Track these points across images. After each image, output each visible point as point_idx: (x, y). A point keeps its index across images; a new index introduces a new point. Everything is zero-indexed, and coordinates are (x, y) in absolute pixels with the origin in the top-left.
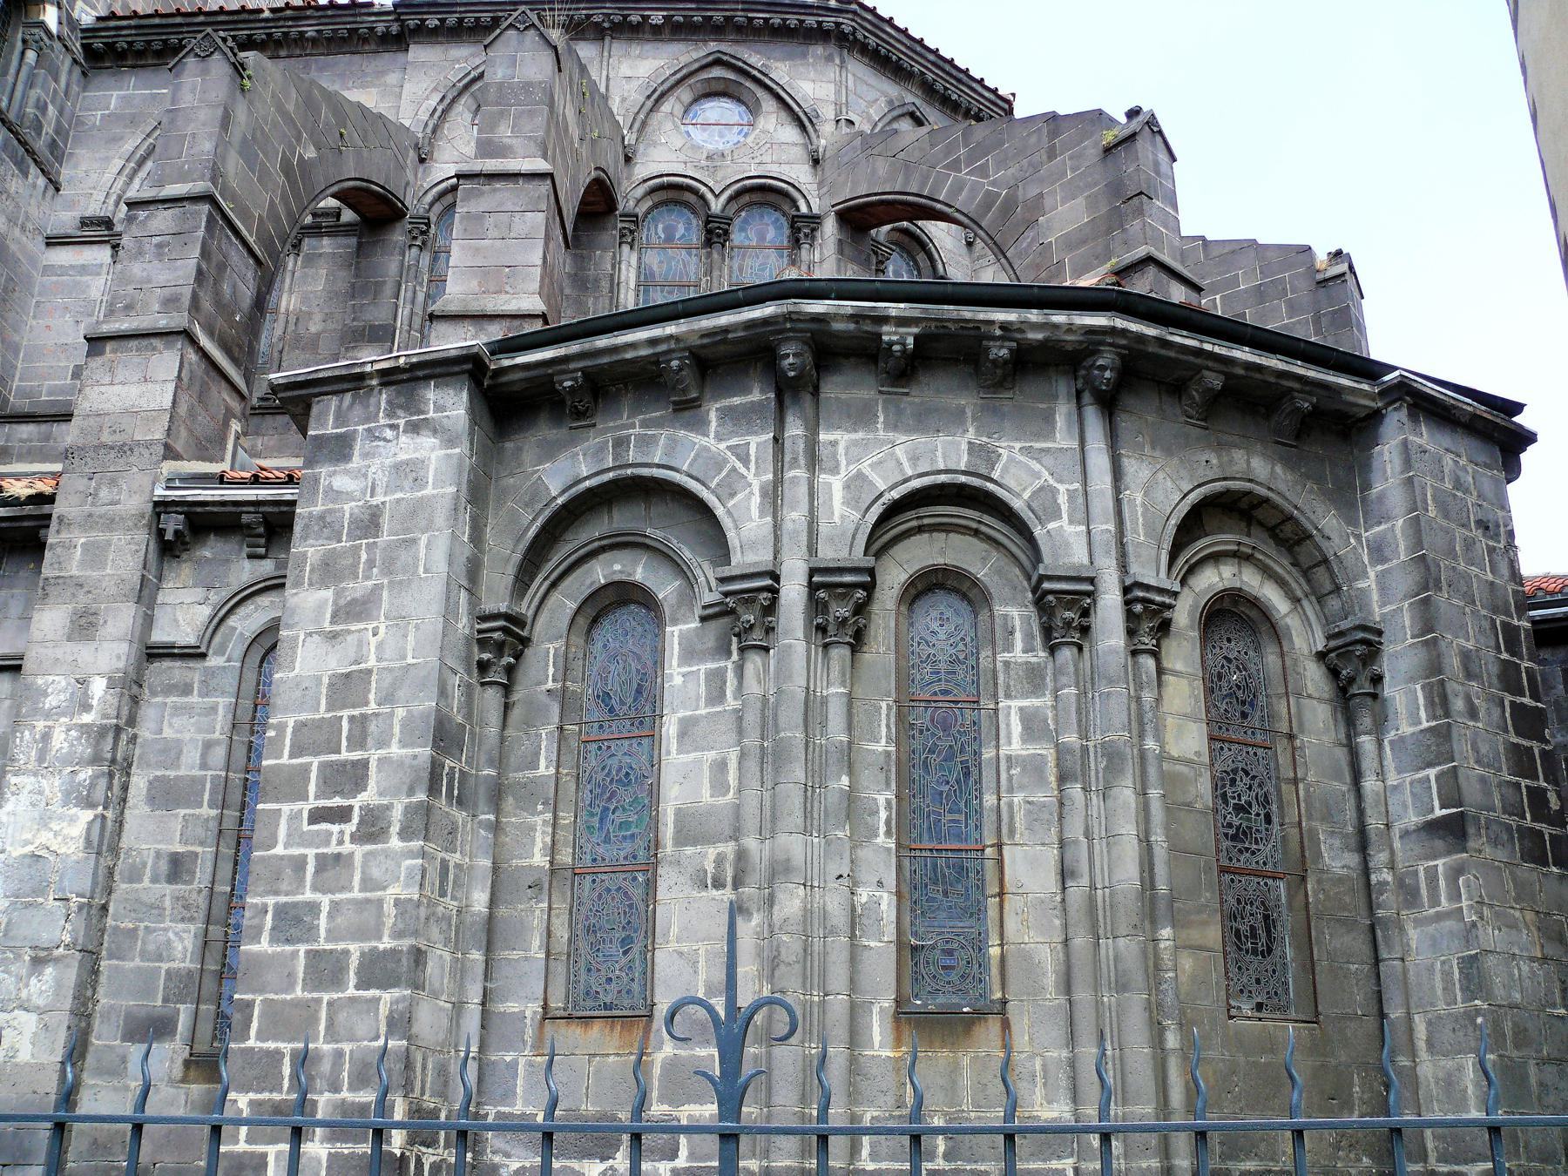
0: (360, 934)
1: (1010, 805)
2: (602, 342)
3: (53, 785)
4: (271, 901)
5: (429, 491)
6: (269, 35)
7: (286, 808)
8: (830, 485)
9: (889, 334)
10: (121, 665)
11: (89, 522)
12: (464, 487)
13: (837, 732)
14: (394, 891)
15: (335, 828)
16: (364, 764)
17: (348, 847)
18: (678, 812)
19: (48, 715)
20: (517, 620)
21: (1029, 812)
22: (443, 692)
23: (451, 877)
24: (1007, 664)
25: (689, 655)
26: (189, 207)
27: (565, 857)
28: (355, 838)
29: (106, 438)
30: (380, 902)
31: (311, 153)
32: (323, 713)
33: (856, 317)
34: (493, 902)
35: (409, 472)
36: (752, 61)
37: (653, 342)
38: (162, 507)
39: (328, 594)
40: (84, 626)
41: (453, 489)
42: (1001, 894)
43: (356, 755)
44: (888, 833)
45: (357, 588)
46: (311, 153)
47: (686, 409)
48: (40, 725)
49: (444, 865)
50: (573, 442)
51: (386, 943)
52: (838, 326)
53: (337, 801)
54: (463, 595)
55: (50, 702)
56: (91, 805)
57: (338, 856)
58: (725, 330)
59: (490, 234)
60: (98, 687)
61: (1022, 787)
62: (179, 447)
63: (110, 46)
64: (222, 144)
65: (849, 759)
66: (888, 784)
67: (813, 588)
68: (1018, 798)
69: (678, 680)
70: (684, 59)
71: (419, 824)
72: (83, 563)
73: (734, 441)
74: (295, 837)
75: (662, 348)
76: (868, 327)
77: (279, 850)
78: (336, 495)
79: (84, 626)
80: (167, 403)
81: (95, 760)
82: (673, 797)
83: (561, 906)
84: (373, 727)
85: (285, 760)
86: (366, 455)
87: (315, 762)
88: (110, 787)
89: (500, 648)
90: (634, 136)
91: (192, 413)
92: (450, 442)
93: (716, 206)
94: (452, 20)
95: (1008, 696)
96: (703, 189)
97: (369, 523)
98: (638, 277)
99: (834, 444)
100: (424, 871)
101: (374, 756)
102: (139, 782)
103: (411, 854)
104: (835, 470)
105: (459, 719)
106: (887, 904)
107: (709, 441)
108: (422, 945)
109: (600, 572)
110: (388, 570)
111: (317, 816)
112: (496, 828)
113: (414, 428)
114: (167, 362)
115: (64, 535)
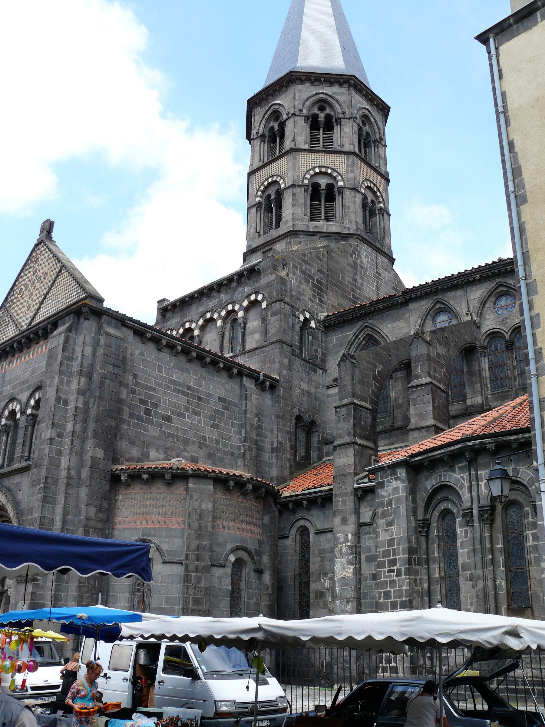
0: (399, 597)
1: (530, 557)
2: (430, 455)
3: (344, 560)
4: (382, 591)
5: (400, 495)
6: (370, 310)
7: (382, 570)
8: (481, 485)
9: (488, 446)
10: (354, 530)
11: (341, 495)
12: (408, 492)
13: (488, 545)
14: (404, 588)
15: (392, 574)
16: (396, 559)
17: (395, 578)
18: (462, 564)
19: (341, 544)
20: (427, 520)
21: (535, 559)
22: (409, 541)
23: (418, 582)
24: (528, 522)
25: (461, 527)
26: (348, 407)
27: (443, 574)
28: (396, 576)
29: (341, 473)
30: (402, 590)
31: (381, 367)
32: (387, 548)
33: (480, 444)
34: (429, 586)
35: (396, 490)
36: (510, 282)
37: (440, 454)
38: (356, 489)
39: (384, 520)
41: (405, 494)
42: (530, 579)
43: (394, 557)
44: (503, 567)
45: (390, 518)
46: (381, 367)
47: (451, 468)
49: (416, 580)
50: (431, 476)
51: (404, 599)
52: (476, 447)
53: (392, 568)
54: (412, 517)
55: (340, 540)
56: (352, 564)
57: (393, 580)
58: (453, 450)
59: (419, 403)
61: (533, 553)
62: (358, 471)
63: (330, 324)
64: (353, 385)
65: (492, 551)
66: (502, 554)
67: (480, 511)
68: (532, 555)
69: (459, 532)
70: (489, 288)
71: (407, 572)
72: (341, 506)
73: (461, 475)
74: (385, 577)
75: (442, 455)
76: (483, 446)
77: (382, 579)
78: (383, 497)
79: (344, 521)
80: (353, 462)
82: (461, 561)
83: (443, 586)
84: (396, 551)
85: (381, 559)
86: (387, 486)
87: (387, 559)
88: (356, 560)
89: (423, 527)
90: (479, 319)
91: (360, 461)
92: (403, 482)
93: (507, 336)
94: (419, 294)
95: (529, 530)
96: (503, 332)
97: (390, 503)
98: (489, 365)
99: (482, 474)
100: (410, 583)
101: (398, 557)
102: (363, 557)
103: (406, 579)
104: (482, 481)
105: (415, 546)
106: (504, 583)
107: (456, 475)
108: (411, 598)
109: (442, 506)
110: (395, 515)
112: (428, 569)
113: (396, 479)
114: (350, 451)
115: (337, 499)
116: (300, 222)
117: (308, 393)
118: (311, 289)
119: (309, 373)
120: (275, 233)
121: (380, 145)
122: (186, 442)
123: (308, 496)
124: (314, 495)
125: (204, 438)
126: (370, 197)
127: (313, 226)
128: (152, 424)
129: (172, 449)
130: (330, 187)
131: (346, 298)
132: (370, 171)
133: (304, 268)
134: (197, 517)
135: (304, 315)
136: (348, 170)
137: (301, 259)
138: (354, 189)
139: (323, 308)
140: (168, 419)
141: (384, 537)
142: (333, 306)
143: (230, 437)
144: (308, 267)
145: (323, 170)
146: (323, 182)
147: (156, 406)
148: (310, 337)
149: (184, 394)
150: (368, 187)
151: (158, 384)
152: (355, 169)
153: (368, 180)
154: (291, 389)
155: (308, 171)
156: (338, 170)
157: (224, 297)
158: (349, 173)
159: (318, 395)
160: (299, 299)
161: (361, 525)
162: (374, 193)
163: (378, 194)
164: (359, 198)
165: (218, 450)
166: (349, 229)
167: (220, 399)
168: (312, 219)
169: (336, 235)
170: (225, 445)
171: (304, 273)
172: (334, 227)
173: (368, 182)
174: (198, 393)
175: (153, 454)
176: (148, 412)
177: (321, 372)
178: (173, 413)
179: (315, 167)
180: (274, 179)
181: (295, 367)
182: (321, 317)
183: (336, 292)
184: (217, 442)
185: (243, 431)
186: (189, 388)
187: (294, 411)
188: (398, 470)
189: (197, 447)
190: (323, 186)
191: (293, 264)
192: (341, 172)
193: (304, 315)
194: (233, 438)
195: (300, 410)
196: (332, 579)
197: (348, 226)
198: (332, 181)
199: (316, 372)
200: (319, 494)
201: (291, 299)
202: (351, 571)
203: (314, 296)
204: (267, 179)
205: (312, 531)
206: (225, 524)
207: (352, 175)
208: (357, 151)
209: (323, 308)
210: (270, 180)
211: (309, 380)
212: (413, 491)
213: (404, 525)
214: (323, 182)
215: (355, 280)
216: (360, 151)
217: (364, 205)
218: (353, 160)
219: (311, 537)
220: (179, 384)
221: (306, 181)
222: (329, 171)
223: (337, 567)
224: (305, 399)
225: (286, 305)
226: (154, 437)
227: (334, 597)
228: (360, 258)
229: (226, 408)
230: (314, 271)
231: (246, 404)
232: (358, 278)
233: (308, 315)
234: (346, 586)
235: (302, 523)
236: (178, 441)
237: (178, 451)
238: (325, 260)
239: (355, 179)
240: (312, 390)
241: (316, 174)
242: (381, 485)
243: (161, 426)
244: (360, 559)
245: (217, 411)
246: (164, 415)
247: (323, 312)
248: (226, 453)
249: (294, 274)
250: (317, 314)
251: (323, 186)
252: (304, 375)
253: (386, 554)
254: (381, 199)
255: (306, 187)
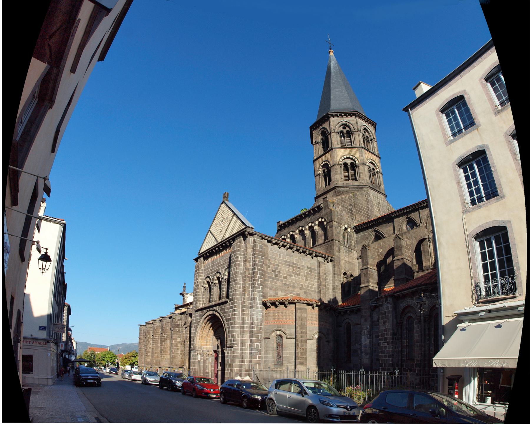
16: (387, 337)
19: (364, 330)
22: (393, 330)
35: (387, 308)
39: (382, 321)
40: (366, 320)
41: (391, 309)
45: (385, 320)
48: (364, 331)
51: (390, 354)
53: (385, 341)
55: (364, 328)
56: (369, 339)
60: (368, 326)
78: (382, 310)
79: (366, 320)
80: (369, 294)
81: (369, 334)
97: (385, 313)
102: (374, 336)
111: (384, 342)
113: (388, 303)
116: (340, 182)
117: (349, 262)
118: (347, 214)
119: (348, 253)
120: (329, 188)
121: (374, 141)
122: (294, 287)
123: (350, 309)
124: (352, 309)
125: (302, 285)
126: (372, 166)
127: (346, 183)
128: (278, 280)
129: (288, 290)
130: (352, 164)
131: (364, 216)
132: (371, 154)
133: (343, 205)
134: (300, 320)
135: (344, 226)
136: (360, 155)
137: (341, 200)
138: (364, 164)
139: (353, 222)
140: (285, 278)
141: (382, 328)
142: (358, 221)
143: (314, 284)
144: (345, 204)
145: (348, 156)
146: (349, 162)
147: (280, 272)
148: (348, 236)
149: (292, 266)
150: (370, 162)
151: (280, 263)
152: (363, 154)
153: (369, 159)
154: (340, 261)
155: (341, 157)
156: (355, 156)
157: (308, 219)
158: (360, 157)
159: (353, 263)
160: (341, 219)
161: (373, 322)
162: (374, 165)
163: (376, 165)
164: (366, 168)
165: (309, 290)
166: (363, 183)
167: (308, 268)
168: (345, 180)
169: (357, 187)
170: (312, 288)
171: (343, 206)
172: (356, 183)
173: (370, 160)
174: (298, 266)
175: (280, 293)
176: (276, 275)
177: (354, 252)
178: (287, 275)
179: (344, 156)
180: (326, 162)
181: (342, 251)
182: (353, 226)
183: (359, 214)
184: (308, 286)
185: (319, 281)
186: (294, 263)
187: (342, 271)
188: (389, 299)
189: (299, 289)
190: (349, 164)
191: (338, 203)
192: (357, 157)
193: (344, 226)
194: (315, 285)
195: (345, 270)
196: (361, 345)
197: (362, 182)
198: (353, 162)
199: (351, 252)
200: (355, 308)
201: (338, 219)
202: (369, 341)
203: (349, 217)
204: (322, 163)
205: (351, 324)
206: (313, 322)
207: (362, 158)
208: (363, 146)
209: (353, 222)
210: (324, 163)
211: (349, 256)
212: (395, 308)
213: (391, 323)
214: (349, 162)
215: (368, 207)
216: (365, 146)
217: (370, 171)
218: (362, 151)
219: (351, 326)
220: (289, 262)
221: (340, 163)
222: (351, 157)
223: (363, 340)
224: (347, 265)
225: (336, 223)
226: (280, 286)
227: (362, 352)
228: (370, 196)
229: (311, 271)
230: (347, 205)
231: (320, 269)
232: (369, 206)
233: (346, 226)
234: (366, 348)
235: (347, 320)
236: (290, 287)
237: (291, 291)
238: (353, 200)
239: (363, 159)
240: (351, 261)
241: (345, 159)
242: (381, 305)
243: (282, 281)
244: (373, 336)
245: (307, 273)
246: (283, 276)
247: (354, 224)
248: (312, 291)
249: (338, 207)
250: (351, 225)
251: (349, 164)
252: (346, 254)
253: (383, 335)
254: (377, 167)
255: (341, 165)
